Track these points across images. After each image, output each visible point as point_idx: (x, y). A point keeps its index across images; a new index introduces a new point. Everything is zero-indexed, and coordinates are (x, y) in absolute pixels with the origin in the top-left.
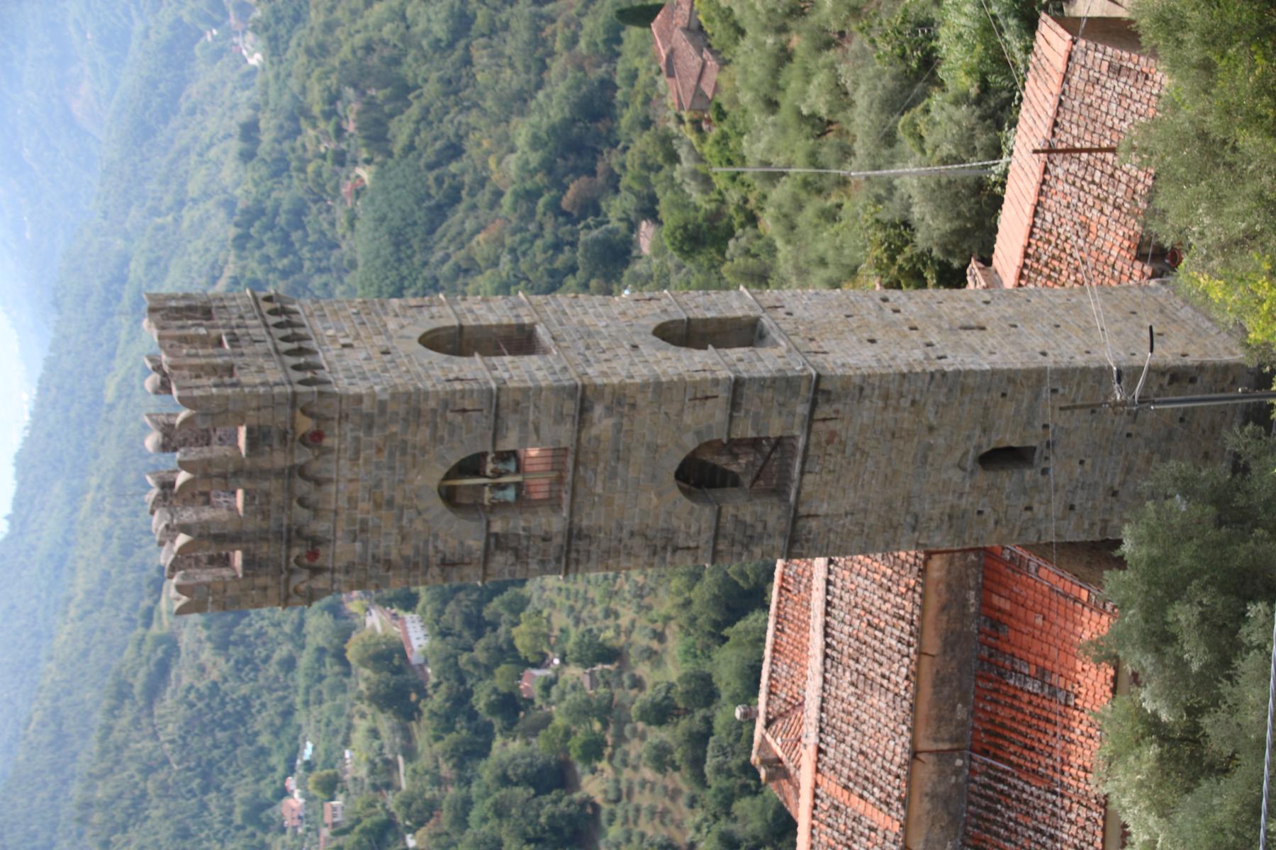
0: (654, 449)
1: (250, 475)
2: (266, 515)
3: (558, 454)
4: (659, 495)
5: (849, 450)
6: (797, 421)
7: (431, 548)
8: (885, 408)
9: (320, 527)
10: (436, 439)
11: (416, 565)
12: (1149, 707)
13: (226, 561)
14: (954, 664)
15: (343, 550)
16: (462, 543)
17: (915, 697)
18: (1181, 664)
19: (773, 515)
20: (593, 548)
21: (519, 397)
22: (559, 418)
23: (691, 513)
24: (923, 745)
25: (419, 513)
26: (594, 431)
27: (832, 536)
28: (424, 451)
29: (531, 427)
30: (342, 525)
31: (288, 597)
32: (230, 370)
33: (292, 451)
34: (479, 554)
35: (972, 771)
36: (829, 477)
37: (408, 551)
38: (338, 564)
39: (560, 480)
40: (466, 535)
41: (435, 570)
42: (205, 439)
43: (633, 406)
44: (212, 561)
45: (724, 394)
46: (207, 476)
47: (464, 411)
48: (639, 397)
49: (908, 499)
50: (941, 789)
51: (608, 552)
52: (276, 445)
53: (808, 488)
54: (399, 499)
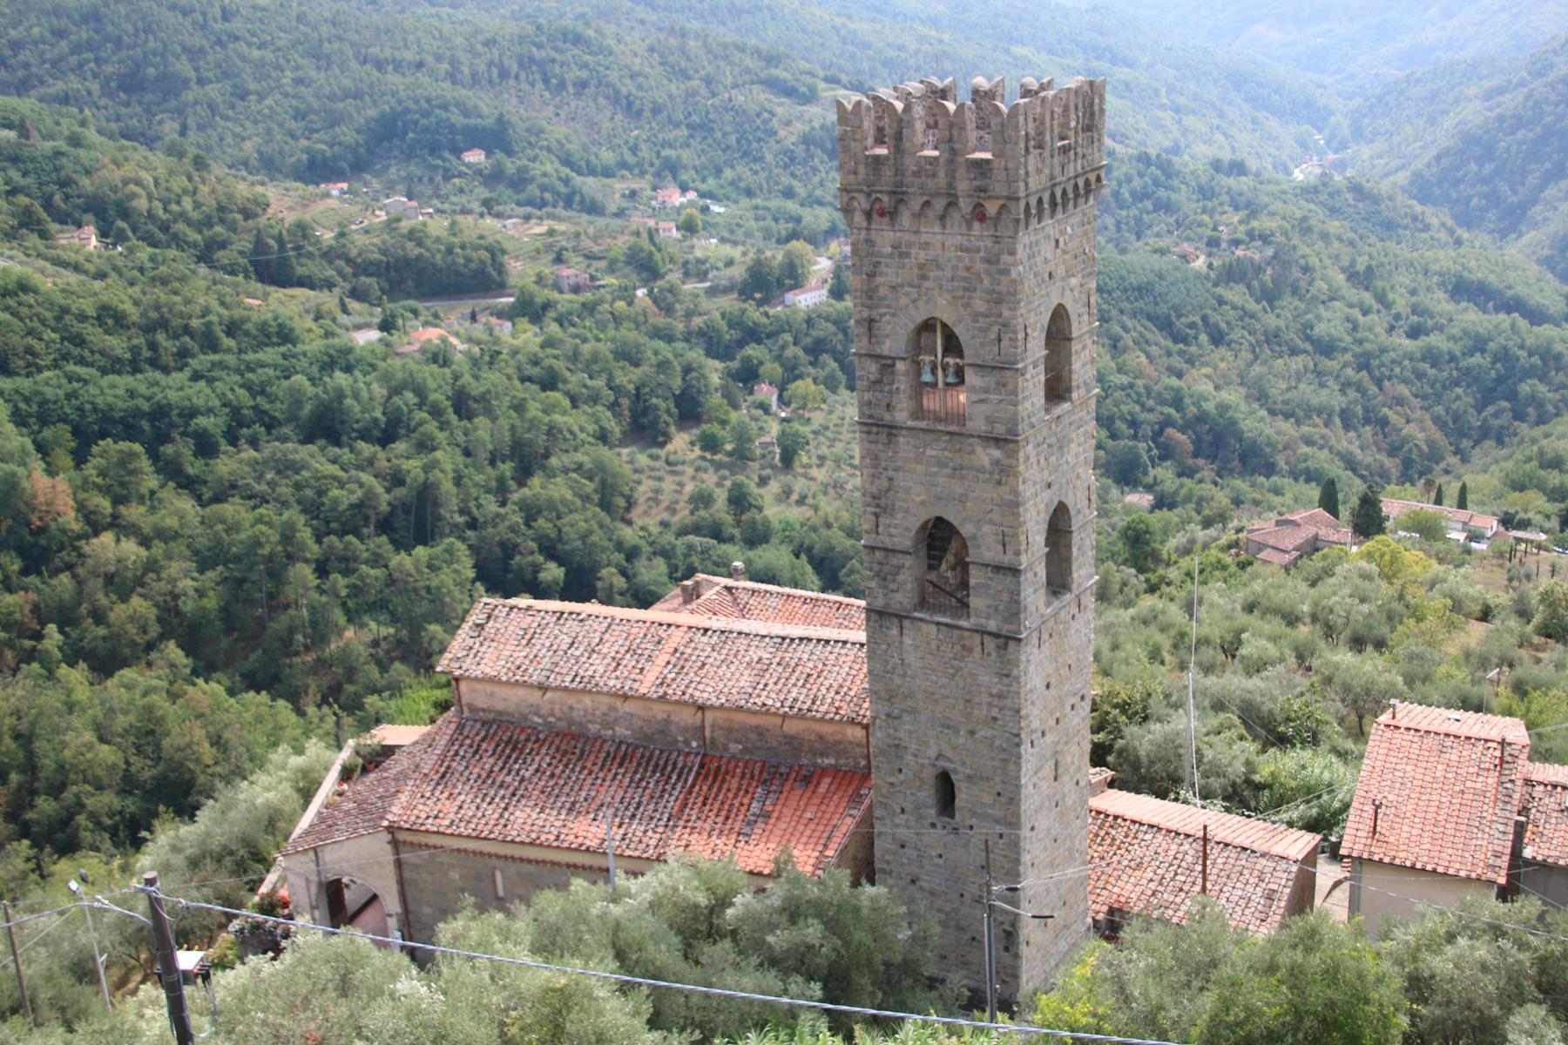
0: (962, 499)
1: (951, 162)
2: (916, 174)
3: (961, 419)
4: (923, 503)
5: (956, 663)
6: (983, 621)
8: (991, 695)
9: (905, 219)
10: (976, 316)
11: (871, 298)
12: (738, 900)
13: (879, 141)
14: (775, 744)
15: (885, 237)
16: (887, 336)
17: (749, 711)
18: (772, 927)
19: (903, 598)
20: (880, 446)
21: (1010, 387)
22: (991, 420)
23: (907, 529)
24: (709, 715)
25: (914, 301)
26: (979, 449)
28: (966, 306)
29: (984, 396)
30: (906, 237)
31: (848, 191)
32: (1040, 146)
33: (969, 196)
34: (878, 351)
35: (688, 754)
36: (933, 646)
37: (882, 292)
39: (938, 419)
40: (894, 340)
41: (865, 314)
42: (982, 125)
43: (999, 483)
44: (880, 130)
45: (1007, 559)
46: (951, 126)
47: (1000, 340)
48: (1007, 488)
49: (913, 711)
50: (673, 728)
51: (876, 458)
52: (975, 183)
53: (925, 627)
54: (926, 284)
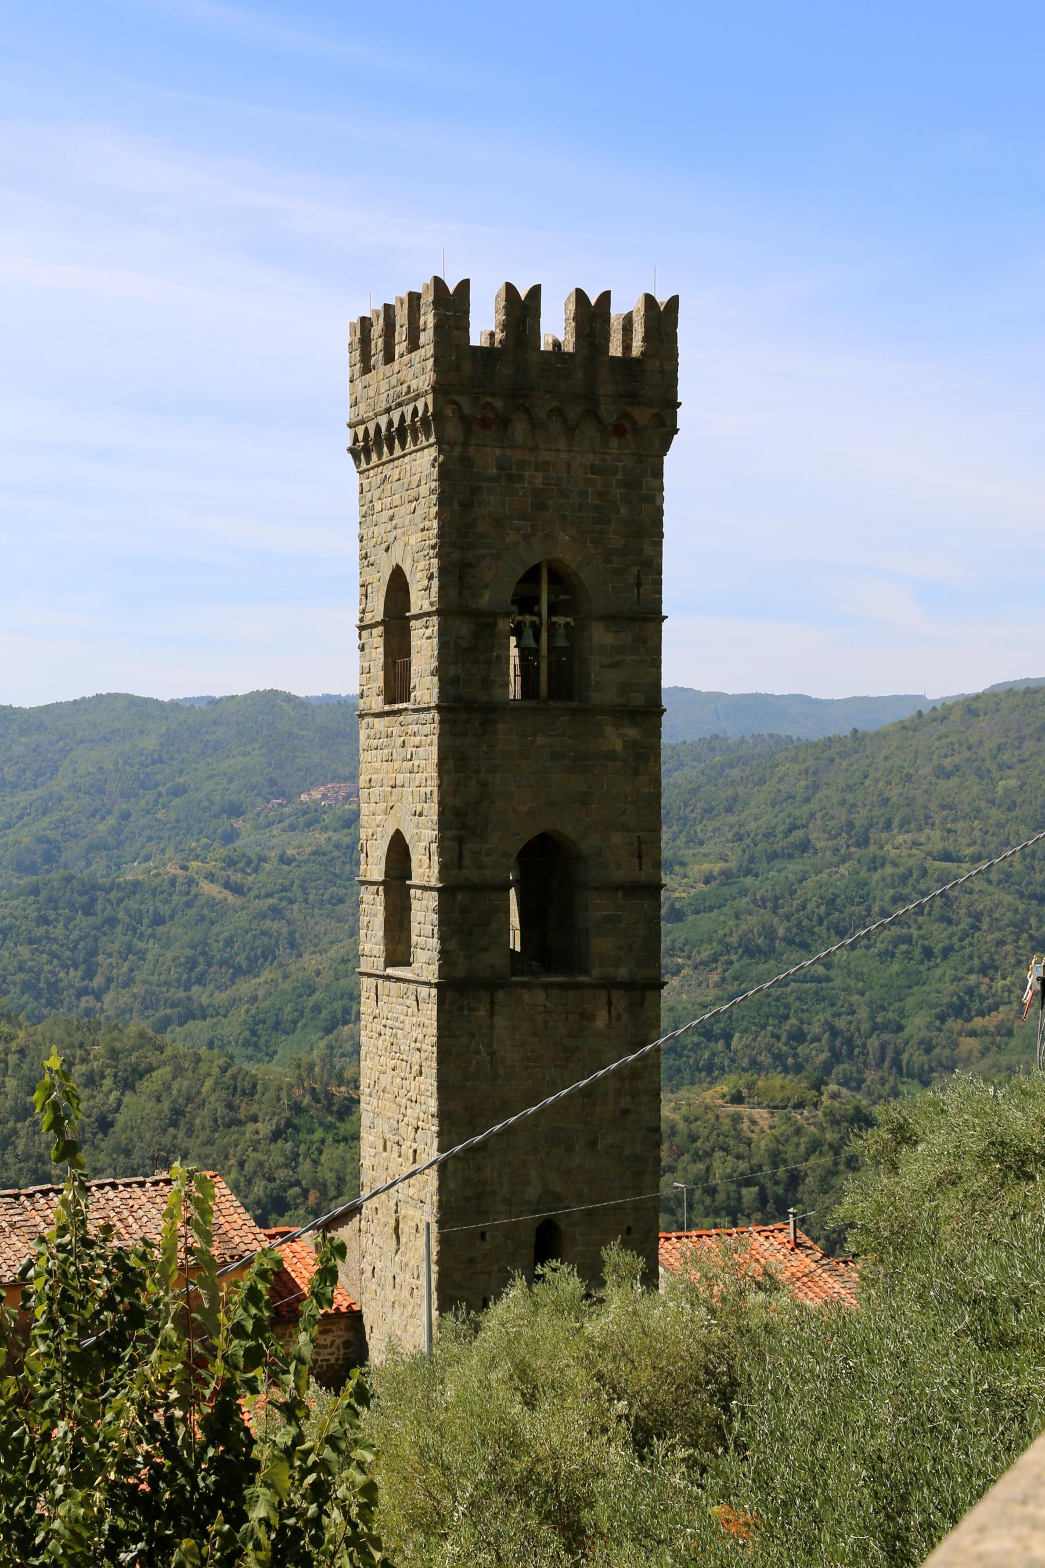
7: (484, 551)
9: (520, 429)
15: (488, 457)
26: (609, 730)
27: (464, 1040)
38: (472, 451)
41: (456, 556)
43: (636, 773)
45: (643, 876)
47: (639, 585)
53: (527, 997)
